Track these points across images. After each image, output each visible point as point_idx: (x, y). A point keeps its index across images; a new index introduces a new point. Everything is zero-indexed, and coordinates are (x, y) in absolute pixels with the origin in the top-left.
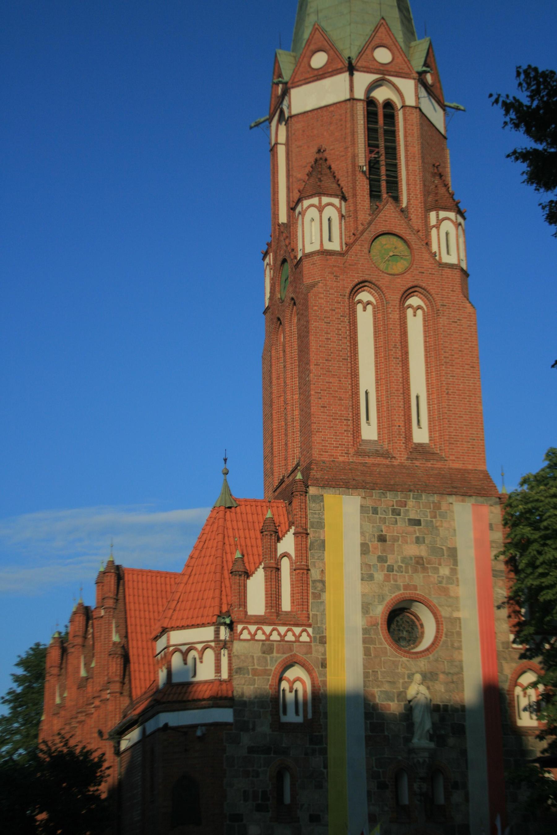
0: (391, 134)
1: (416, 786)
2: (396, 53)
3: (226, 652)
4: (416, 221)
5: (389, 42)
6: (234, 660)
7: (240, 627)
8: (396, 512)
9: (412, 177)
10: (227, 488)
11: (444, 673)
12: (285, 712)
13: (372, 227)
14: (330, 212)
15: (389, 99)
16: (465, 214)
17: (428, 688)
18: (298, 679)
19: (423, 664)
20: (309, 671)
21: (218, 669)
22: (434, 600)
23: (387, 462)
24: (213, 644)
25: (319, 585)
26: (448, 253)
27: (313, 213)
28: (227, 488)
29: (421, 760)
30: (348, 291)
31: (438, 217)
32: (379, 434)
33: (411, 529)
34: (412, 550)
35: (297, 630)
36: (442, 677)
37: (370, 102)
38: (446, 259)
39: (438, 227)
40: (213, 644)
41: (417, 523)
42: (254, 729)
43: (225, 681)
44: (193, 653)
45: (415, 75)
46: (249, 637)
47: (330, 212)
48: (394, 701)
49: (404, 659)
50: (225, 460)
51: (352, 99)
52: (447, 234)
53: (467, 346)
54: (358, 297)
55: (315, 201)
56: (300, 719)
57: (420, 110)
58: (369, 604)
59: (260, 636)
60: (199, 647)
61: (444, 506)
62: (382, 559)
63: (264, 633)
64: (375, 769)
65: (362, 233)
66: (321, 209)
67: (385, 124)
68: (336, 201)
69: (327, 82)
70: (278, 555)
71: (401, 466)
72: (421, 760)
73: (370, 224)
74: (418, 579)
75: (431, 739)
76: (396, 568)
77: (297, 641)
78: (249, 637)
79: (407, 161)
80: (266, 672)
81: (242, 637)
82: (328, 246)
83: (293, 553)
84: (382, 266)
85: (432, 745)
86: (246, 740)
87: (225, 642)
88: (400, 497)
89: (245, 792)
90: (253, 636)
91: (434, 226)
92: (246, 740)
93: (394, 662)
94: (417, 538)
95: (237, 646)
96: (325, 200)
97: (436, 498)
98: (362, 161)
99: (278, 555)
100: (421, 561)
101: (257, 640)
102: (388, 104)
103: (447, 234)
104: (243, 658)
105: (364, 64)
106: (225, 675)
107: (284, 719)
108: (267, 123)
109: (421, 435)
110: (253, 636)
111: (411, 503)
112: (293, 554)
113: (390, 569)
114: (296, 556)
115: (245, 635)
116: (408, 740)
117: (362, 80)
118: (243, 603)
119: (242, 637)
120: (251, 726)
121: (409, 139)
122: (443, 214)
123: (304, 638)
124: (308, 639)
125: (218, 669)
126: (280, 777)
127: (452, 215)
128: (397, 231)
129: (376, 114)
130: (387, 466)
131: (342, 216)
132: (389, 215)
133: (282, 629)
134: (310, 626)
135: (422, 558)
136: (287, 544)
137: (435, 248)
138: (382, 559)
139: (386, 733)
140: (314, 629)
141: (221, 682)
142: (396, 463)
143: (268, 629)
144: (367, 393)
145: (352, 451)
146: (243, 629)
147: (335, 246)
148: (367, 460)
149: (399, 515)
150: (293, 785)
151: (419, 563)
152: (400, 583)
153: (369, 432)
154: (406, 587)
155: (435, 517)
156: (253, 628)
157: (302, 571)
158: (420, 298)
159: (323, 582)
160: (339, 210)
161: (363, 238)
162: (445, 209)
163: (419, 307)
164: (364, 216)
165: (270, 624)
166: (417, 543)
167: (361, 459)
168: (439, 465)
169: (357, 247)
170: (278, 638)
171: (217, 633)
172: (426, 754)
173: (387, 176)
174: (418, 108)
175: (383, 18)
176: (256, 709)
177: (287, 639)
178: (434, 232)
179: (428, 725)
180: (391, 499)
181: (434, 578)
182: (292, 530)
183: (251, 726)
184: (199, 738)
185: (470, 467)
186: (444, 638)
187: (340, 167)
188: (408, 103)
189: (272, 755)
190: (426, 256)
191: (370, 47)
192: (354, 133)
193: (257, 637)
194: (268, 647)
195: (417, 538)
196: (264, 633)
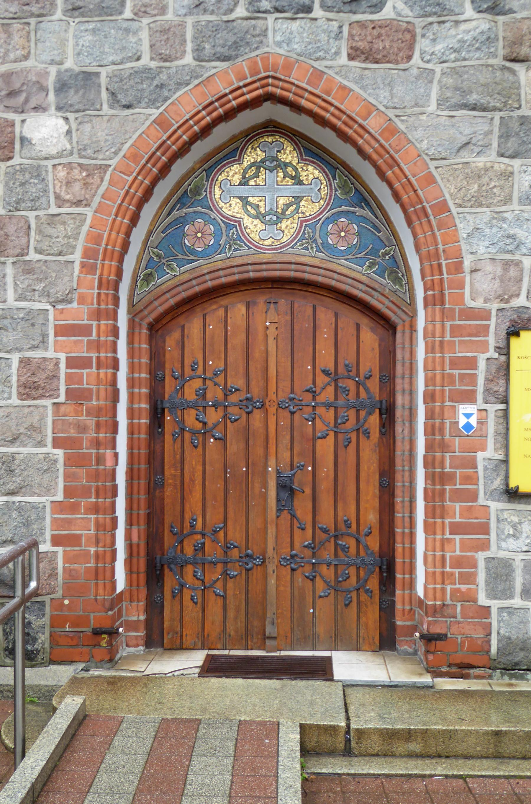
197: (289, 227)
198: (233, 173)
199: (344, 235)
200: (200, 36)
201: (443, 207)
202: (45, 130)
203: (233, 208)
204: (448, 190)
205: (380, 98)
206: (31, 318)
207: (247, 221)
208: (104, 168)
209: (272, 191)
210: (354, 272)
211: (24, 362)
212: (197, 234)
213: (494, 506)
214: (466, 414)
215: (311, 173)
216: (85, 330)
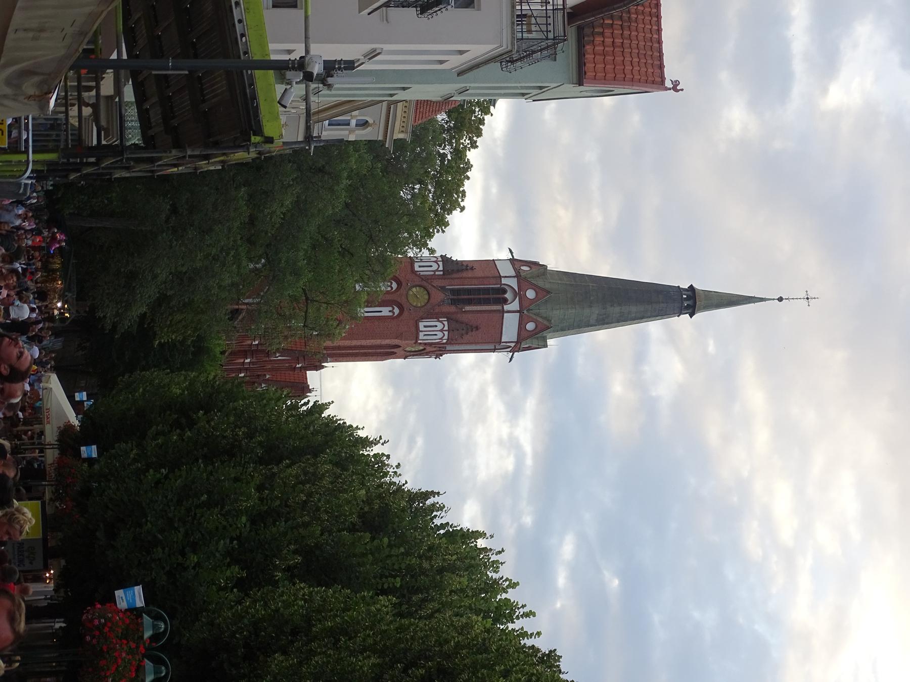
14: (435, 267)
26: (425, 327)
37: (505, 292)
39: (439, 321)
68: (441, 268)
96: (441, 264)
102: (505, 301)
122: (446, 323)
127: (446, 328)
147: (417, 268)
160: (437, 270)
164: (435, 283)
174: (503, 312)
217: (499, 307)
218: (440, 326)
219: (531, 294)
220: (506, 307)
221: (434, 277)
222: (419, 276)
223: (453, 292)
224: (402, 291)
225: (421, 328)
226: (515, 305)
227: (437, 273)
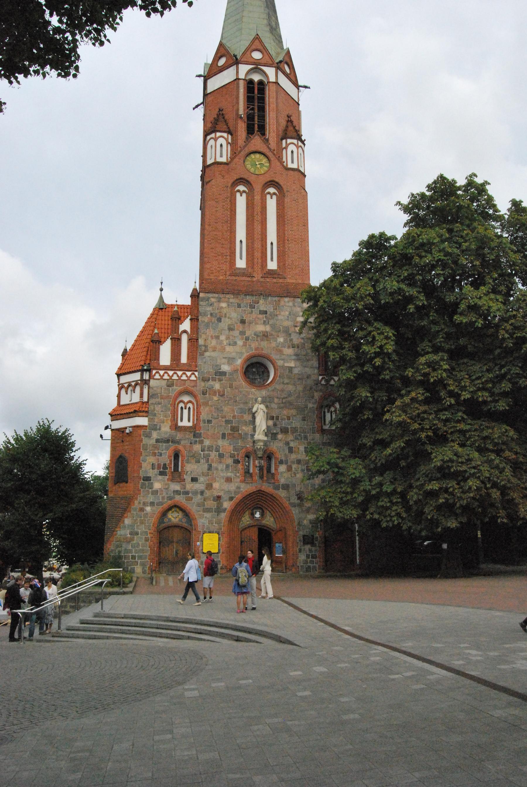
0: (262, 100)
1: (257, 462)
2: (265, 53)
3: (147, 387)
4: (273, 144)
5: (260, 47)
6: (151, 390)
7: (154, 372)
8: (252, 307)
9: (272, 121)
10: (161, 297)
11: (277, 398)
12: (182, 420)
13: (246, 149)
15: (261, 80)
16: (305, 142)
17: (267, 407)
18: (190, 402)
19: (264, 393)
20: (195, 396)
21: (142, 396)
22: (274, 356)
23: (249, 279)
24: (139, 382)
25: (203, 348)
26: (292, 162)
27: (212, 142)
28: (161, 297)
29: (259, 447)
30: (230, 185)
31: (286, 142)
32: (247, 264)
33: (261, 316)
34: (261, 328)
35: (189, 373)
36: (276, 400)
37: (251, 82)
38: (290, 165)
39: (286, 148)
40: (139, 382)
41: (265, 312)
42: (160, 429)
43: (145, 402)
44: (130, 388)
45: (276, 65)
46: (159, 377)
47: (221, 141)
48: (245, 414)
49: (253, 390)
50: (162, 283)
51: (238, 79)
52: (292, 152)
53: (301, 214)
54: (237, 188)
55: (213, 135)
56: (190, 424)
57: (278, 84)
58: (234, 358)
59: (166, 377)
60: (133, 384)
61: (282, 303)
62: (242, 333)
63: (169, 375)
64: (232, 452)
65: (240, 152)
66: (216, 139)
67: (258, 94)
68: (225, 135)
69: (225, 73)
70: (180, 331)
71: (258, 281)
72: (259, 447)
73: (245, 146)
74: (264, 344)
75: (266, 435)
76: (250, 338)
77: (188, 379)
78: (159, 377)
79: (269, 112)
80: (168, 397)
81: (155, 377)
82: (219, 159)
83: (189, 330)
84: (252, 170)
85: (265, 438)
86: (155, 435)
87: (145, 380)
88: (254, 298)
89: (153, 464)
90: (162, 377)
91: (284, 148)
92: (155, 435)
93: (247, 391)
94: (264, 321)
95: (152, 382)
96: (218, 134)
97: (277, 299)
98: (241, 112)
99: (180, 331)
100: (266, 334)
101: (165, 379)
102: (261, 83)
103: (292, 152)
104: (155, 389)
105: (245, 60)
106: (145, 399)
107: (180, 424)
108: (202, 105)
109: (272, 265)
110: (162, 377)
111: (261, 301)
112: (189, 330)
113: (247, 339)
114: (191, 332)
115: (157, 376)
116: (253, 436)
117: (244, 69)
118: (157, 358)
119: (155, 377)
120: (158, 428)
121: (271, 100)
122: (289, 141)
123: (193, 378)
124: (195, 379)
125: (142, 396)
126: (176, 456)
127: (295, 141)
128: (261, 150)
129: (253, 88)
130: (249, 281)
131: (228, 143)
132: (257, 142)
133: (180, 373)
134: (196, 371)
135: (267, 332)
136: (186, 325)
137: (284, 159)
138: (242, 333)
139: (240, 432)
140: (199, 372)
141: (143, 403)
142: (254, 279)
143: (171, 373)
144: (241, 241)
145: (228, 273)
146: (157, 372)
147: (224, 160)
148: (237, 278)
149: (254, 308)
150: (182, 460)
151: (265, 336)
152: (253, 346)
153: (241, 263)
154: (257, 349)
155: (276, 309)
156: (162, 372)
157: (193, 341)
158: (275, 188)
159: (206, 346)
160: (227, 140)
161: (240, 154)
162: (292, 138)
163: (274, 194)
165: (172, 370)
166: (264, 324)
167: (234, 278)
168: (281, 281)
169: (236, 160)
170: (177, 378)
171: (142, 375)
172: (262, 444)
173: (258, 122)
174: (277, 83)
175: (258, 35)
176: (162, 417)
177: (182, 378)
178: (284, 151)
179: (264, 427)
180: (249, 299)
181: (274, 344)
182: (189, 318)
183: (158, 428)
184: (127, 433)
185: (300, 282)
186: (278, 378)
187: (230, 116)
188: (270, 81)
189: (170, 444)
190: (278, 164)
191: (249, 51)
192: (237, 98)
193: (164, 378)
194: (170, 383)
195: (264, 321)
196: (169, 375)
197: (177, 519)
198: (170, 512)
199: (184, 520)
200: (167, 497)
201: (196, 518)
202: (148, 509)
203: (170, 517)
204: (197, 517)
205: (189, 506)
206: (146, 532)
207: (172, 518)
208: (155, 514)
209: (175, 514)
210: (185, 525)
211: (145, 538)
212: (166, 520)
213: (201, 554)
214: (198, 543)
215: (180, 512)
216: (152, 533)
217: (273, 88)
218: (291, 148)
219: (257, 55)
220: (272, 79)
221: (233, 144)
222: (232, 159)
223: (250, 131)
224: (252, 179)
225: (295, 166)
226: (271, 72)
227: (230, 141)
